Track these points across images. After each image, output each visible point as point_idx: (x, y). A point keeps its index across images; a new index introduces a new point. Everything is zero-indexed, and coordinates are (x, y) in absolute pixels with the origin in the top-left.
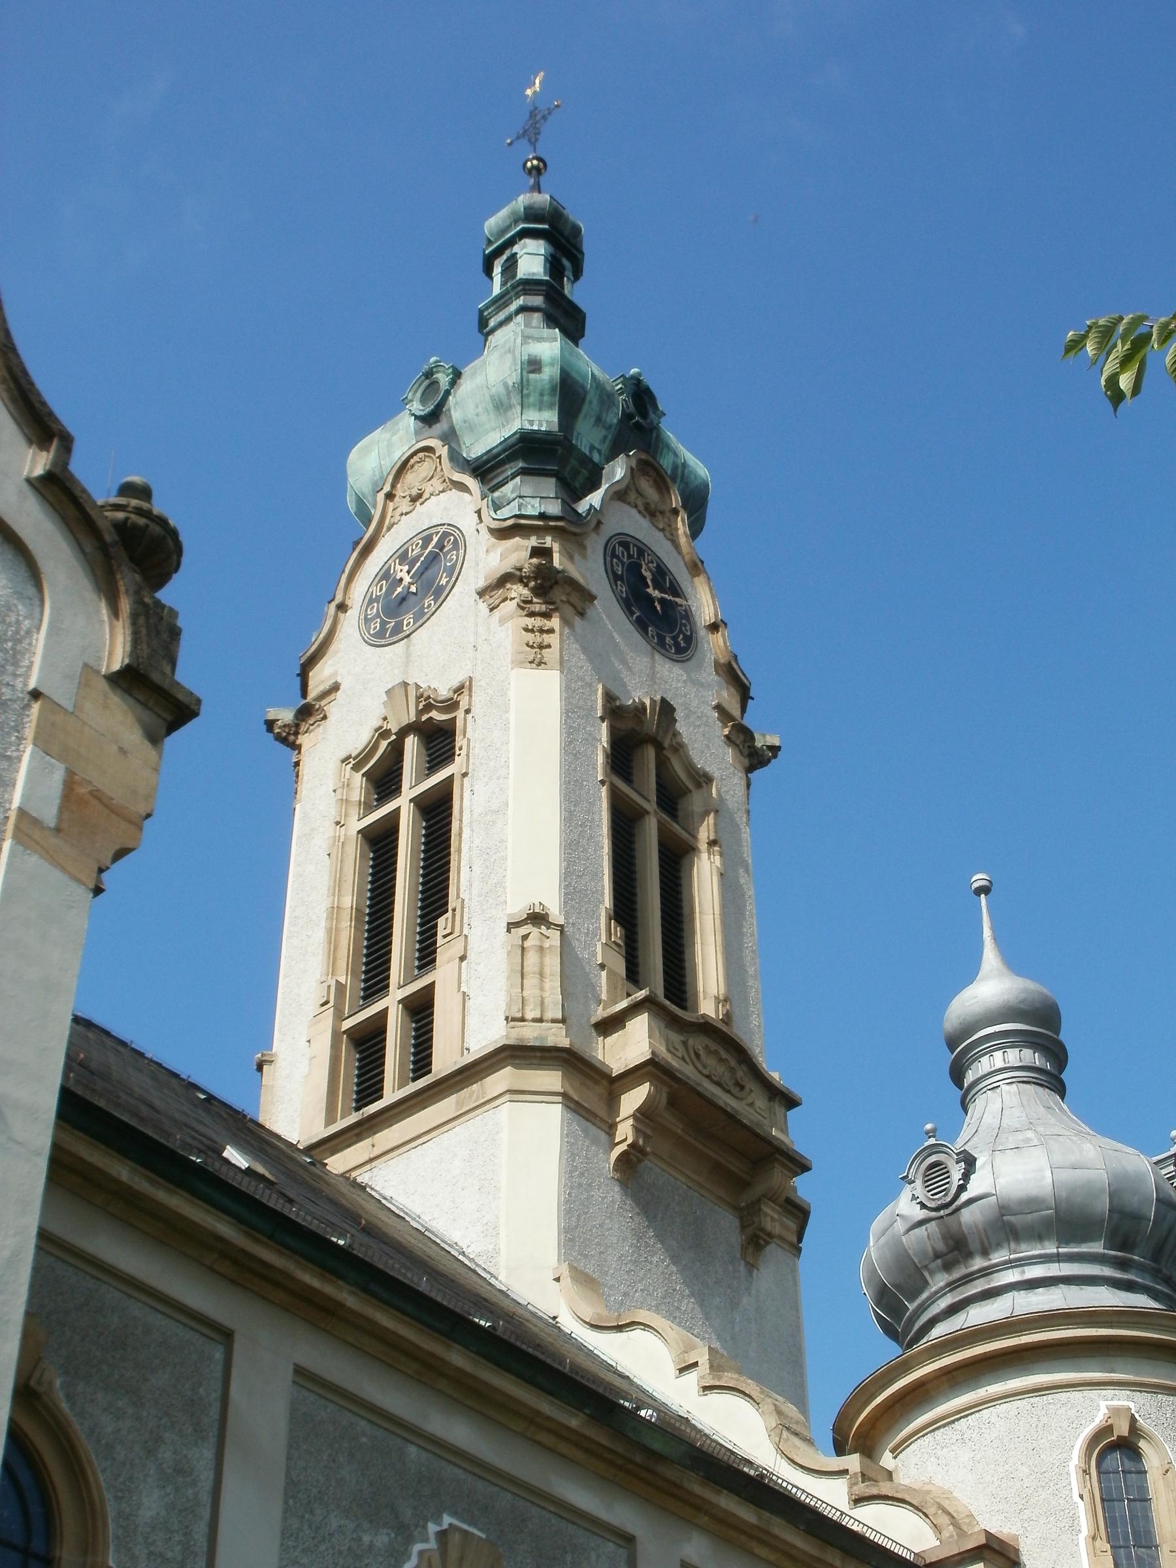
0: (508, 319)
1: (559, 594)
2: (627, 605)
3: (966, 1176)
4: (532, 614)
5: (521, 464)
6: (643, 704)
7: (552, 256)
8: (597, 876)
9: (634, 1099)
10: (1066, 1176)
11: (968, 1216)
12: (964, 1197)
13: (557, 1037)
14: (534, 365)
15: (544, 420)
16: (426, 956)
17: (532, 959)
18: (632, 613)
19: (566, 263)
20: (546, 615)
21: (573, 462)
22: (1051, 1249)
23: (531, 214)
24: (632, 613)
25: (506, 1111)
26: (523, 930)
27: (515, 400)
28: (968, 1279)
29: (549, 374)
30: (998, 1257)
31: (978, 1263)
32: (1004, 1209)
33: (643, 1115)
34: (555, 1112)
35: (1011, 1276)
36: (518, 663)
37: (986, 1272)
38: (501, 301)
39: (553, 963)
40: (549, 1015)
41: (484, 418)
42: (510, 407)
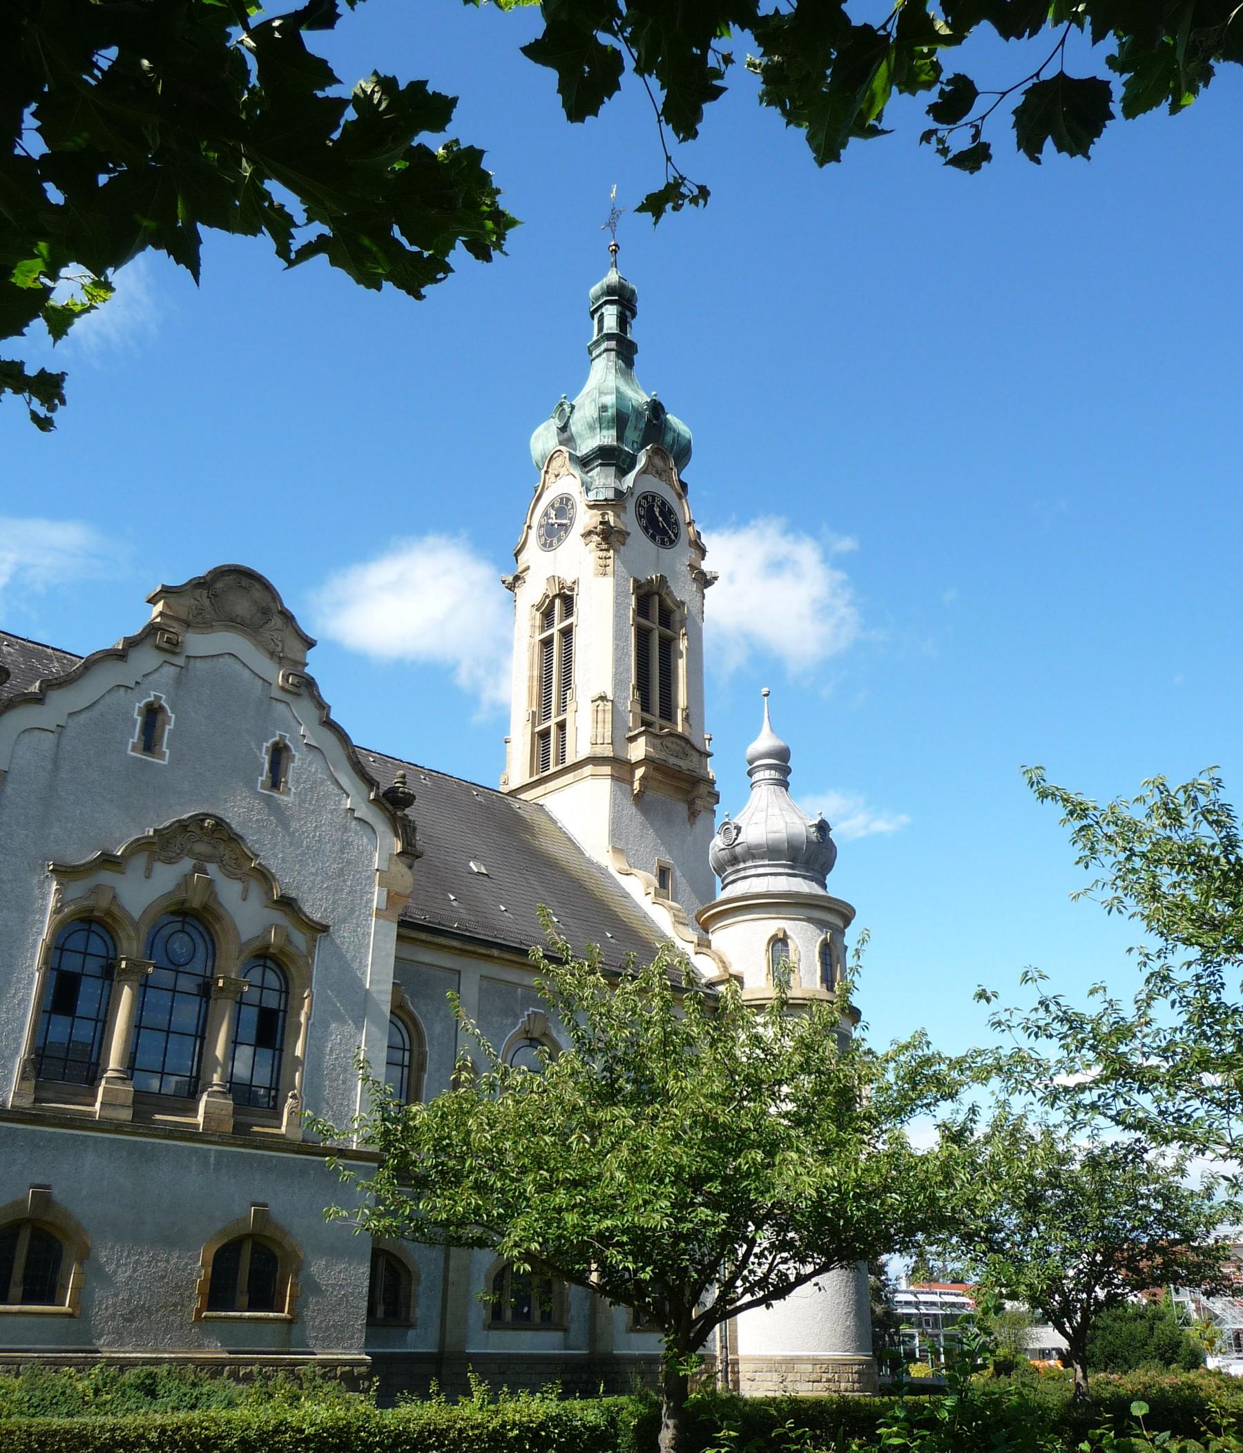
0: (600, 355)
1: (613, 538)
2: (646, 529)
3: (737, 835)
4: (601, 550)
5: (600, 461)
6: (652, 579)
7: (621, 313)
8: (628, 670)
9: (639, 772)
10: (771, 836)
11: (738, 849)
12: (737, 842)
13: (608, 751)
14: (604, 408)
15: (607, 437)
16: (563, 707)
17: (600, 715)
18: (648, 532)
19: (628, 313)
20: (607, 550)
21: (623, 457)
22: (767, 862)
23: (610, 290)
25: (590, 782)
26: (597, 703)
27: (597, 425)
28: (738, 871)
29: (611, 412)
30: (749, 864)
31: (742, 865)
32: (749, 848)
33: (643, 778)
34: (607, 784)
35: (753, 872)
36: (596, 575)
38: (597, 343)
39: (609, 717)
40: (606, 741)
41: (584, 432)
42: (595, 428)
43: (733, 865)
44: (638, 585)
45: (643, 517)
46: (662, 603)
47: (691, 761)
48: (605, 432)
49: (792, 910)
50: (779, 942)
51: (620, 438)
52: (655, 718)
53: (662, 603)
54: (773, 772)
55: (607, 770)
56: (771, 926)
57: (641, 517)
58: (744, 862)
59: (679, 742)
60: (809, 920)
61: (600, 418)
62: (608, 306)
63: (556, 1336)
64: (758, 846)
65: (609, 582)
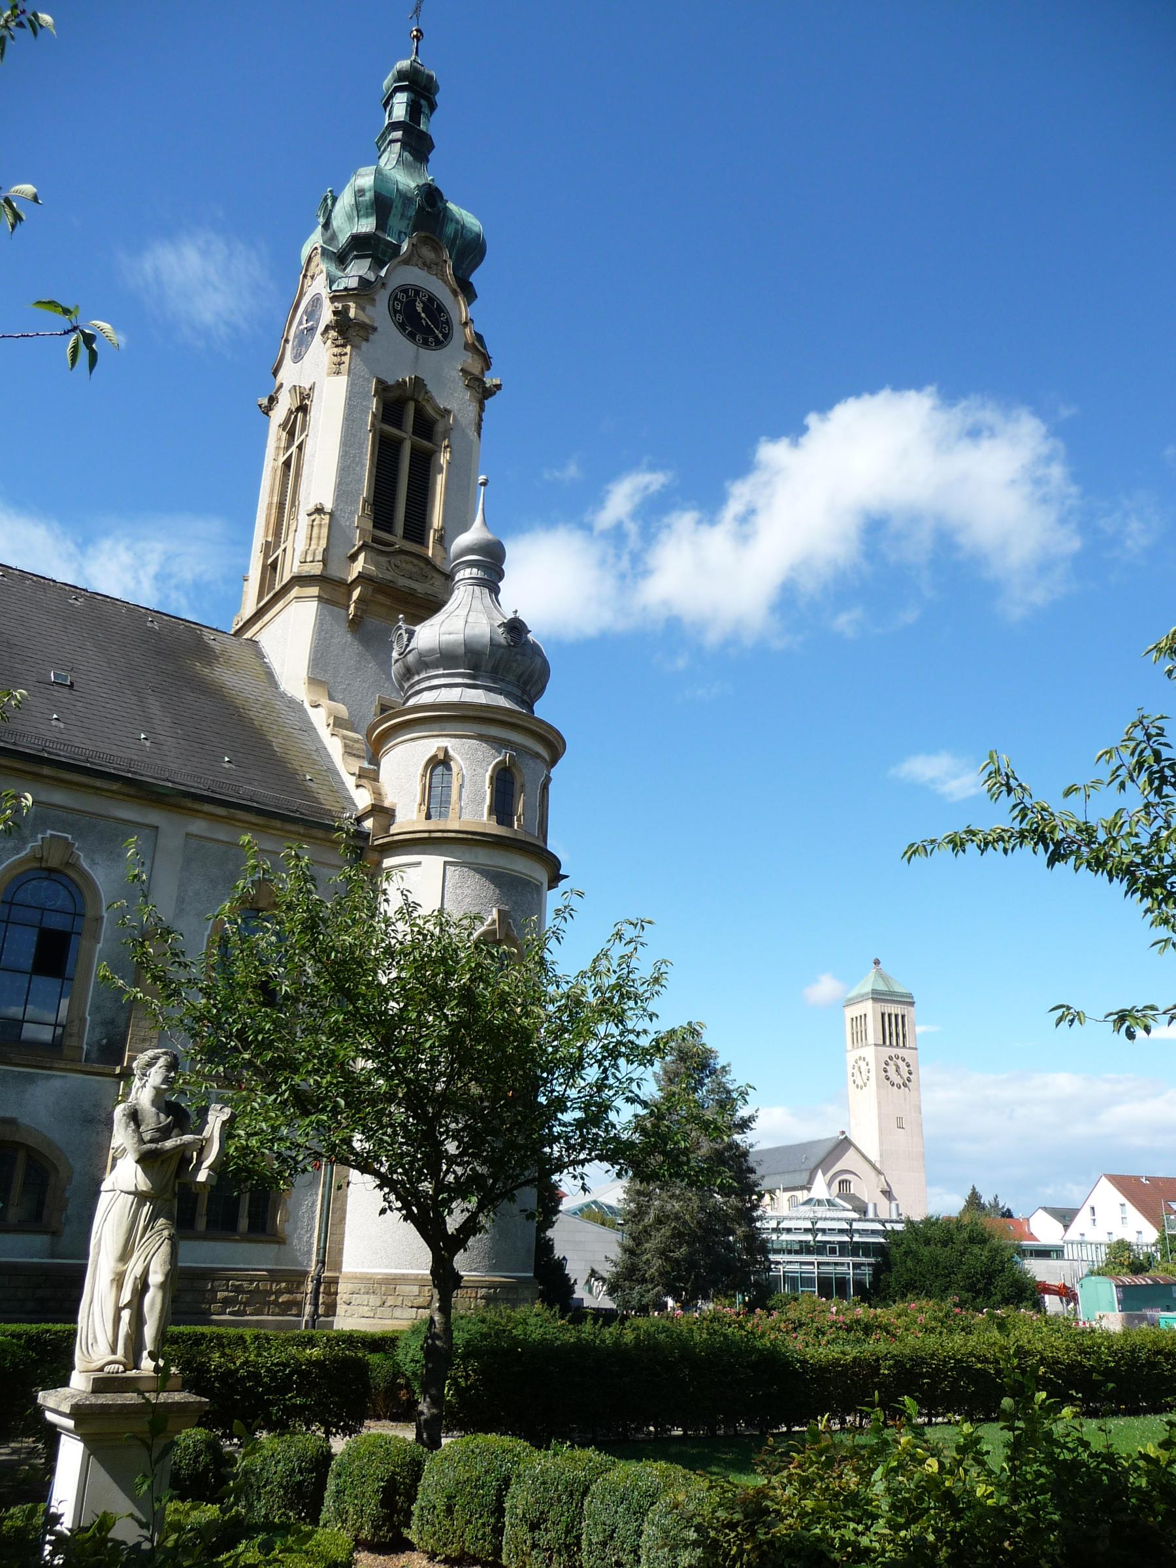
1: (352, 332)
2: (401, 326)
3: (409, 640)
4: (337, 346)
5: (355, 253)
6: (404, 382)
7: (412, 101)
8: (361, 481)
9: (356, 594)
13: (316, 569)
15: (367, 225)
17: (316, 530)
18: (405, 330)
19: (423, 102)
20: (344, 346)
21: (382, 246)
22: (441, 672)
24: (405, 330)
25: (295, 605)
26: (313, 517)
29: (369, 196)
30: (423, 676)
31: (416, 678)
33: (360, 600)
34: (314, 605)
36: (329, 374)
37: (419, 682)
39: (325, 531)
40: (317, 559)
41: (344, 225)
43: (408, 679)
44: (383, 388)
45: (399, 312)
46: (419, 413)
47: (433, 584)
48: (363, 221)
49: (459, 725)
50: (440, 763)
51: (381, 225)
52: (398, 540)
53: (419, 413)
54: (475, 570)
55: (314, 591)
56: (428, 746)
57: (396, 312)
58: (418, 674)
59: (416, 562)
60: (481, 737)
61: (357, 205)
62: (398, 94)
63: (39, 1241)
64: (431, 652)
65: (343, 381)
